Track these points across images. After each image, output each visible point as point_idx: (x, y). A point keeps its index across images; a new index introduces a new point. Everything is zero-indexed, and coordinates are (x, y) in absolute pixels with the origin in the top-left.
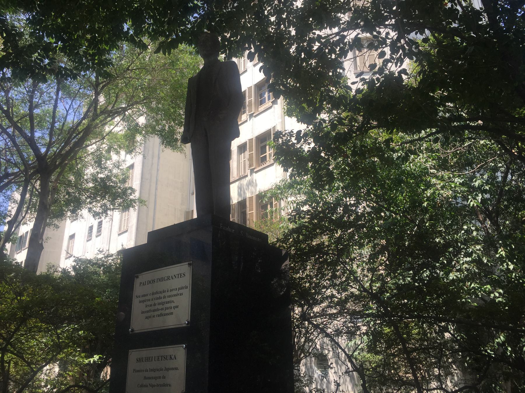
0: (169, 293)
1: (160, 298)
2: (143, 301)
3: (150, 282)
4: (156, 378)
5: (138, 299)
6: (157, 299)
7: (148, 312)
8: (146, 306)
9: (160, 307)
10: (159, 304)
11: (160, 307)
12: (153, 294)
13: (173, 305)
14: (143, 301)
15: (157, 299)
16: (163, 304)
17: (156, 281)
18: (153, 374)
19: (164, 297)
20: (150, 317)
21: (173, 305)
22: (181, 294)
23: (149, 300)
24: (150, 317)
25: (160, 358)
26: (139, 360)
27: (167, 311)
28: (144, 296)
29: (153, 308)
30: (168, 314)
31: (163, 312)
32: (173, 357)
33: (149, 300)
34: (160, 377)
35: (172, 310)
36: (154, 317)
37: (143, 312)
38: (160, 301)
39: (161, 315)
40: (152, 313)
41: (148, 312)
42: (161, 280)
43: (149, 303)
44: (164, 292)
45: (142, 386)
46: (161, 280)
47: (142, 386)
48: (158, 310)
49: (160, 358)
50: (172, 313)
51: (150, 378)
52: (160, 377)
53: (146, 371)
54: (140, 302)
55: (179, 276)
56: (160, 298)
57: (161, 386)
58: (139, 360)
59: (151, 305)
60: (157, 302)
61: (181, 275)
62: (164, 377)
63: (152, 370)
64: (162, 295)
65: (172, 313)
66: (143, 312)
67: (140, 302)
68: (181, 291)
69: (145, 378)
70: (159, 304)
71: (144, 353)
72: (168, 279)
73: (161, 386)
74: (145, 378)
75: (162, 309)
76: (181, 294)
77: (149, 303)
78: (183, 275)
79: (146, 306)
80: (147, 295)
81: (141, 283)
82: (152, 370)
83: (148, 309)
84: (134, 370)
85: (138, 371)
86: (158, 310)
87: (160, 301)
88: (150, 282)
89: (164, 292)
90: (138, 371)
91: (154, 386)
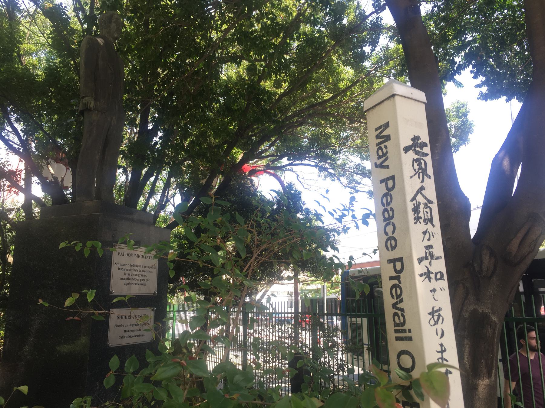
2: (122, 270)
3: (128, 255)
4: (133, 331)
6: (134, 270)
7: (127, 279)
8: (125, 274)
10: (136, 275)
11: (137, 277)
12: (131, 265)
14: (122, 270)
15: (134, 270)
18: (131, 328)
20: (128, 284)
21: (146, 278)
22: (151, 272)
24: (128, 284)
26: (120, 317)
28: (122, 265)
29: (130, 277)
34: (137, 330)
37: (122, 279)
38: (137, 273)
41: (127, 279)
43: (127, 272)
45: (122, 337)
47: (122, 337)
50: (145, 285)
51: (129, 331)
53: (126, 326)
54: (119, 269)
57: (138, 336)
58: (120, 317)
59: (129, 275)
60: (134, 273)
63: (130, 325)
65: (145, 285)
66: (122, 279)
67: (119, 269)
68: (151, 270)
69: (125, 331)
70: (136, 275)
71: (125, 312)
73: (138, 336)
74: (125, 331)
75: (138, 280)
76: (151, 272)
77: (127, 272)
79: (125, 274)
80: (125, 265)
81: (119, 253)
82: (130, 325)
83: (126, 277)
84: (115, 325)
85: (119, 326)
88: (128, 255)
90: (119, 326)
91: (133, 337)
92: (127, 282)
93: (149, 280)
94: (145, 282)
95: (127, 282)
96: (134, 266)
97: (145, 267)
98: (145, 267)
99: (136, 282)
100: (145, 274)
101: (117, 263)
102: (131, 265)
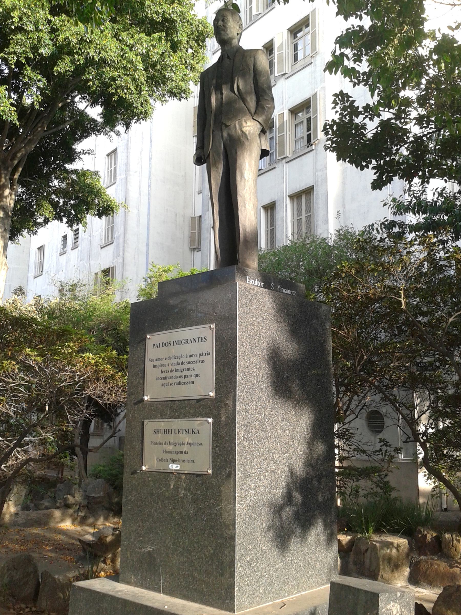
0: (189, 359)
1: (178, 364)
2: (158, 366)
3: (165, 344)
5: (152, 364)
6: (174, 364)
7: (164, 378)
8: (162, 372)
9: (178, 374)
10: (177, 370)
11: (178, 374)
13: (193, 373)
14: (158, 366)
15: (174, 364)
16: (181, 370)
17: (172, 344)
19: (183, 363)
20: (167, 385)
21: (193, 373)
22: (203, 361)
23: (165, 365)
24: (167, 385)
25: (181, 431)
26: (157, 432)
27: (187, 380)
30: (188, 383)
31: (183, 380)
32: (196, 431)
33: (165, 365)
35: (193, 379)
36: (171, 384)
37: (158, 379)
38: (178, 367)
39: (180, 383)
40: (171, 381)
41: (164, 378)
42: (179, 343)
43: (164, 369)
44: (182, 357)
46: (179, 343)
48: (175, 377)
49: (181, 431)
50: (192, 382)
51: (170, 452)
52: (182, 452)
54: (155, 366)
55: (200, 339)
56: (178, 364)
58: (157, 432)
61: (202, 339)
62: (186, 453)
64: (180, 361)
65: (192, 382)
66: (158, 379)
67: (155, 366)
68: (202, 358)
69: (165, 452)
70: (177, 370)
71: (162, 424)
72: (187, 342)
75: (181, 377)
76: (203, 361)
77: (164, 369)
78: (204, 339)
79: (162, 372)
81: (154, 345)
83: (164, 375)
84: (152, 442)
86: (175, 377)
87: (178, 367)
89: (182, 357)
90: (156, 444)
92: (165, 382)
93: (198, 375)
94: (193, 379)
95: (165, 382)
96: (173, 358)
97: (190, 356)
98: (190, 356)
99: (177, 380)
100: (191, 366)
101: (151, 358)
102: (169, 358)
